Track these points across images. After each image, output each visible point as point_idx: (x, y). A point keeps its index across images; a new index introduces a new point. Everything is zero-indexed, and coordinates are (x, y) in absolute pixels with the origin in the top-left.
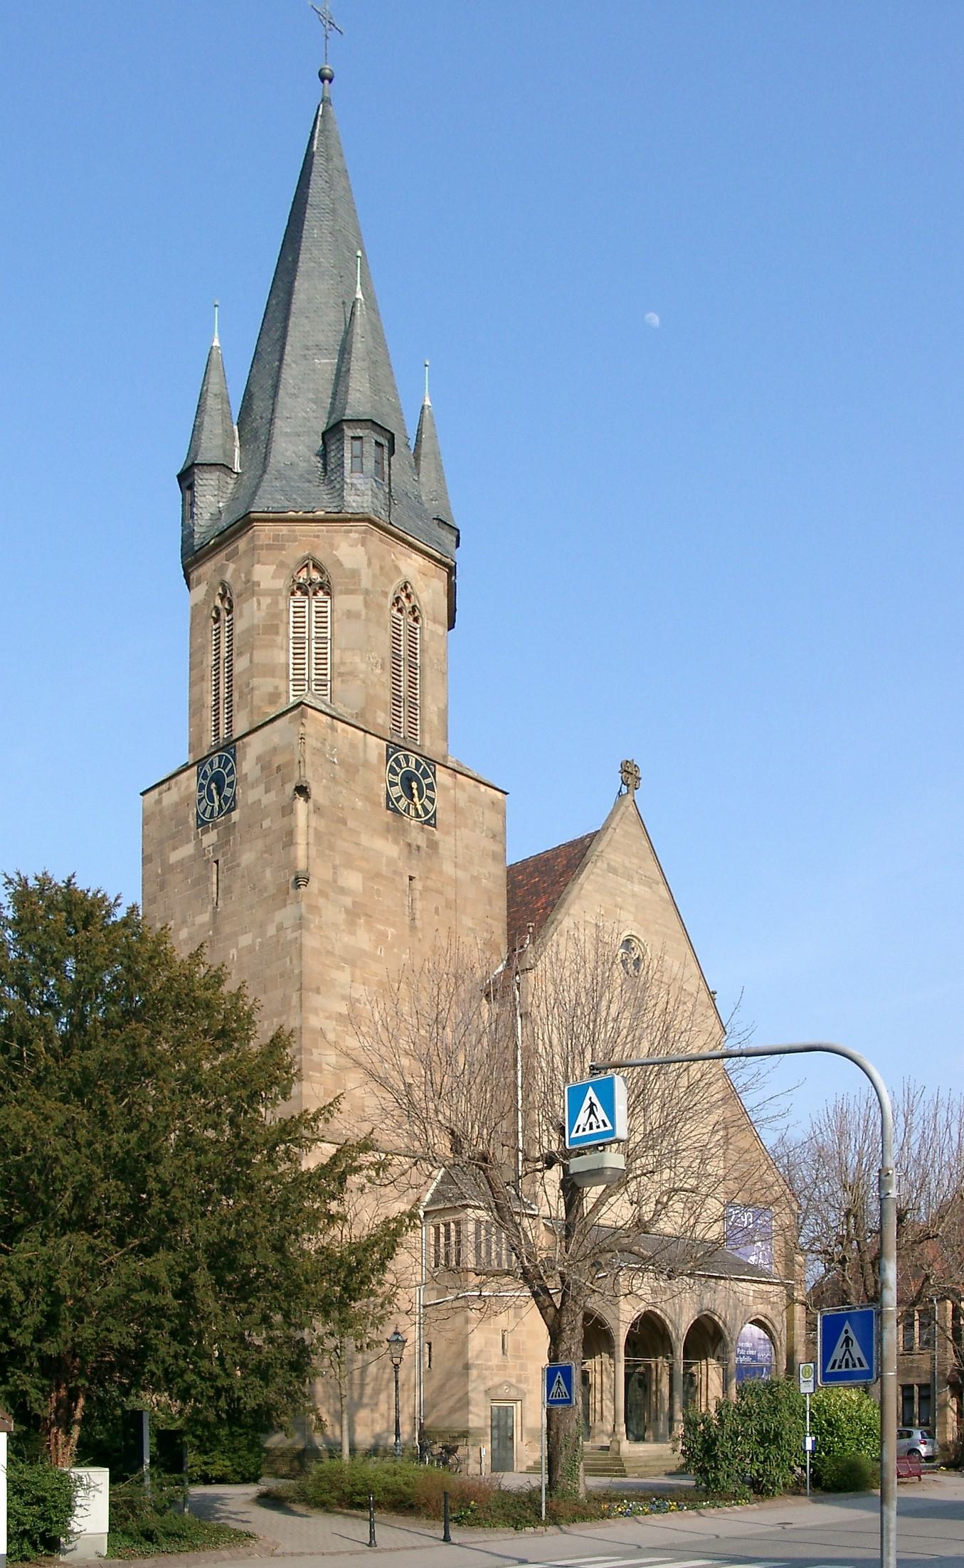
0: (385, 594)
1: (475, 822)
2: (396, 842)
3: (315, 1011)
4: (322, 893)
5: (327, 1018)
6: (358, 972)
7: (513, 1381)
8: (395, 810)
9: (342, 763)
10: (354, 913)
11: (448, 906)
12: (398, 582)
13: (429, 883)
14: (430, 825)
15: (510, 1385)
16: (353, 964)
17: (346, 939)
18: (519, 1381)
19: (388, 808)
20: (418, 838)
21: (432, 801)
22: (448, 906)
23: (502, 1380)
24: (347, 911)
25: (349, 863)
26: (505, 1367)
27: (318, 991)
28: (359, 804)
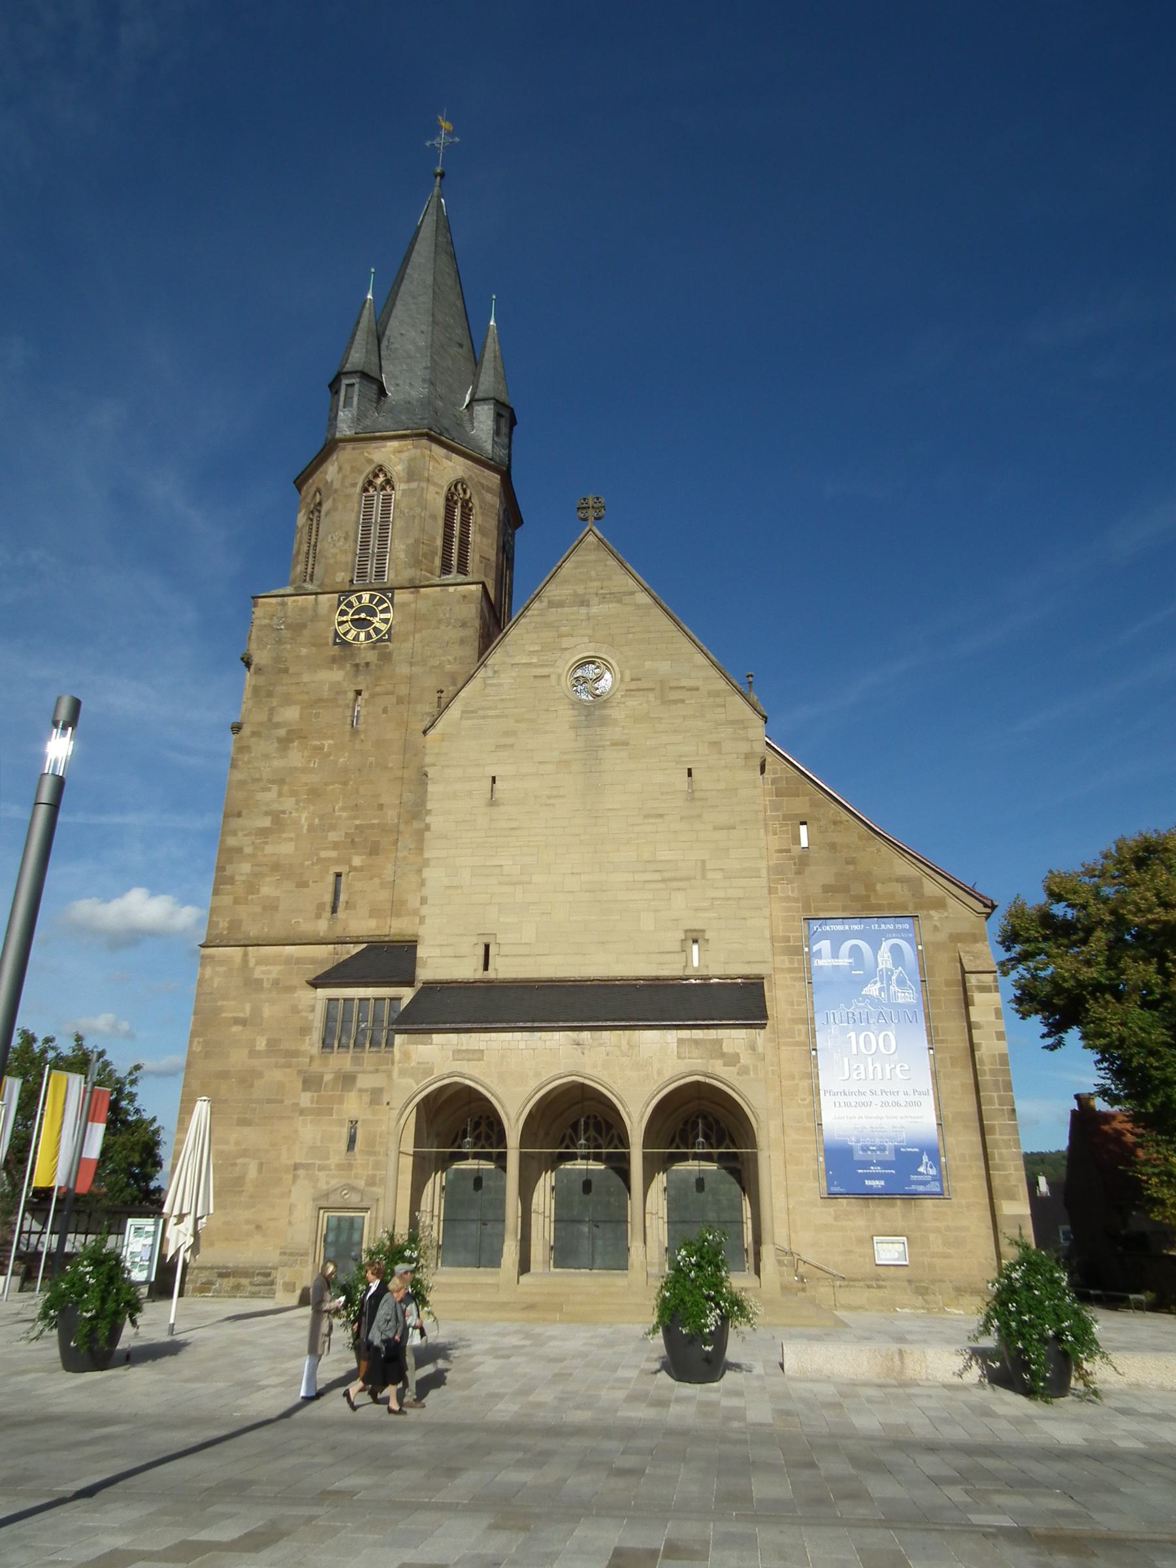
1: (440, 621)
2: (342, 667)
3: (235, 833)
5: (246, 835)
6: (286, 788)
7: (361, 1183)
8: (345, 643)
10: (284, 744)
11: (400, 701)
12: (369, 469)
13: (378, 689)
14: (384, 641)
15: (353, 1189)
16: (281, 782)
18: (371, 1182)
19: (335, 644)
21: (386, 621)
22: (400, 701)
23: (344, 1182)
24: (280, 740)
25: (287, 701)
26: (350, 1167)
27: (239, 815)
28: (304, 651)
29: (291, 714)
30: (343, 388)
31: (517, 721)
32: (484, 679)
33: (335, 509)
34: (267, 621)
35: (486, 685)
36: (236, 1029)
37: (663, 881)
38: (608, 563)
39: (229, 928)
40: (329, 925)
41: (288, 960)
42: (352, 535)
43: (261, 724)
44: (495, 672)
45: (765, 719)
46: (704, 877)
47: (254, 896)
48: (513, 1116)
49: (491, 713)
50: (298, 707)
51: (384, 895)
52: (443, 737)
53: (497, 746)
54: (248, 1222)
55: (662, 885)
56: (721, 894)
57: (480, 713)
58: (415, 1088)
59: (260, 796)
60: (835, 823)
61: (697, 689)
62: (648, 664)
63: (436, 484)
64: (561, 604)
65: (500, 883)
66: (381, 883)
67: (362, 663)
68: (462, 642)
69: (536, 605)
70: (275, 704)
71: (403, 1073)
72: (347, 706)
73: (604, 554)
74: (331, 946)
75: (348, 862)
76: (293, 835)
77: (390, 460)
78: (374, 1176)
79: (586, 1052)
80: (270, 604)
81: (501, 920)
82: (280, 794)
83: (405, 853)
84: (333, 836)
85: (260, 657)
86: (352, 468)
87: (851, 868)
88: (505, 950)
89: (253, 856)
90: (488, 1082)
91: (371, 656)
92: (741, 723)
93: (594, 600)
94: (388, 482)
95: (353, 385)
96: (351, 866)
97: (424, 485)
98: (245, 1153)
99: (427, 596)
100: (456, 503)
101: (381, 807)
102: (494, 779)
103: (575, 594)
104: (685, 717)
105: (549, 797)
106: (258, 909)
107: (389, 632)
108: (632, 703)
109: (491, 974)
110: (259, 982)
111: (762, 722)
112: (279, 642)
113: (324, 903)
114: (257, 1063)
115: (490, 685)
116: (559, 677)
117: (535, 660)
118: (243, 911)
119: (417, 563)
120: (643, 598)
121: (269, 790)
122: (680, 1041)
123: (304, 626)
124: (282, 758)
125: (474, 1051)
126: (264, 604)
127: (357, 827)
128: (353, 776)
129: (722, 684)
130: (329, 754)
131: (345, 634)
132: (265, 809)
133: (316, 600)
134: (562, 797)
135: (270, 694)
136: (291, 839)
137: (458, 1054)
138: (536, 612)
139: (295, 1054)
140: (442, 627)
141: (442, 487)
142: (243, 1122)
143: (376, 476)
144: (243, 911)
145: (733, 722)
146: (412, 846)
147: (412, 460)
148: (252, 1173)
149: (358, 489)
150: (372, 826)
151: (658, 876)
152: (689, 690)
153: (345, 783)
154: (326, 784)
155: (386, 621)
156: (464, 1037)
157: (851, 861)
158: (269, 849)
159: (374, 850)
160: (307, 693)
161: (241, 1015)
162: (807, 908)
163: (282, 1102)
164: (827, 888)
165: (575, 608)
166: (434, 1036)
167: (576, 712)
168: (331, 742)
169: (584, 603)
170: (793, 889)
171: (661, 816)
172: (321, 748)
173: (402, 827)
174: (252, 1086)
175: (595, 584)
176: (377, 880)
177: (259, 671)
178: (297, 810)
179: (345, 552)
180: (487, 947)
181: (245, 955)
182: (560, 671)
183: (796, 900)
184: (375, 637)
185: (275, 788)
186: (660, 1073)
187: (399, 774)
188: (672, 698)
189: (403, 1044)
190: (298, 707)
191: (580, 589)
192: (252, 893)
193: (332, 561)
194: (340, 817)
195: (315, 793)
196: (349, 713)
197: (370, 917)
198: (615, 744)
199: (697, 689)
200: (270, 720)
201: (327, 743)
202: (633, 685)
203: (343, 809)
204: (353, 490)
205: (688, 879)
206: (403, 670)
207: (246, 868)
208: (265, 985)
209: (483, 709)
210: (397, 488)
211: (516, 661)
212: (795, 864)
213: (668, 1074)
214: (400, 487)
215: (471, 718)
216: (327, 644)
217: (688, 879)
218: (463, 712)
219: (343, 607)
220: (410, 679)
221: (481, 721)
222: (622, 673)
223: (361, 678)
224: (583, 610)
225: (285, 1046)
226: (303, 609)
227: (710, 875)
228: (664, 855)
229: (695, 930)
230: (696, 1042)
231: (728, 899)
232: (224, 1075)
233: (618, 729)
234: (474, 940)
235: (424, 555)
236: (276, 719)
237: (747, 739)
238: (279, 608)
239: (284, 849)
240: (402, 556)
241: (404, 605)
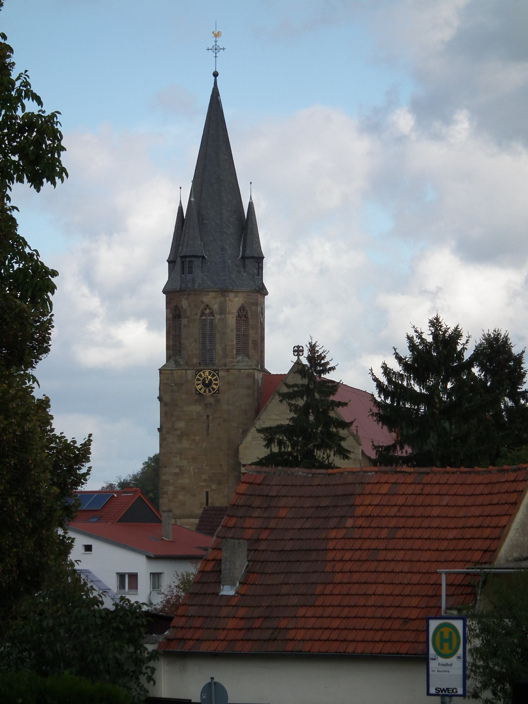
0: (196, 314)
8: (200, 393)
10: (180, 438)
12: (202, 307)
20: (211, 400)
21: (216, 384)
27: (166, 467)
28: (184, 396)
29: (181, 425)
84: (204, 477)
91: (211, 400)
101: (221, 465)
117: (278, 418)
131: (200, 389)
185: (179, 456)
201: (198, 438)
207: (171, 488)
214: (218, 317)
218: (252, 438)
219: (198, 377)
239: (185, 481)
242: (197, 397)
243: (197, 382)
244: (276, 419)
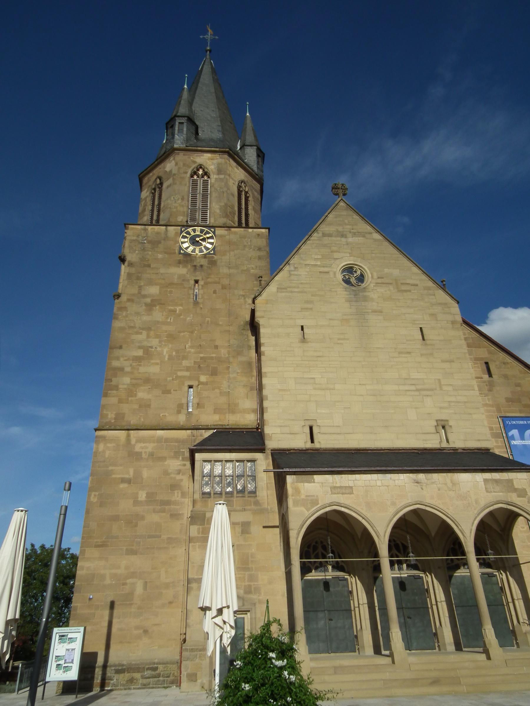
1: (245, 246)
3: (118, 358)
4: (129, 300)
5: (126, 360)
6: (152, 333)
9: (149, 242)
11: (224, 287)
12: (195, 166)
13: (209, 280)
16: (149, 329)
17: (145, 318)
20: (204, 262)
24: (146, 305)
25: (151, 283)
27: (121, 347)
28: (160, 256)
29: (154, 290)
30: (177, 123)
31: (312, 295)
32: (290, 271)
33: (174, 184)
34: (135, 238)
35: (290, 275)
36: (122, 486)
37: (417, 390)
38: (354, 217)
39: (115, 419)
40: (187, 418)
41: (159, 440)
42: (186, 197)
43: (134, 295)
44: (295, 268)
45: (458, 303)
46: (441, 389)
47: (133, 398)
48: (382, 534)
49: (296, 290)
50: (158, 287)
51: (223, 400)
52: (267, 302)
53: (302, 309)
54: (137, 628)
55: (417, 393)
56: (453, 399)
57: (288, 289)
58: (307, 514)
59: (134, 337)
60: (504, 363)
61: (417, 285)
62: (386, 270)
63: (233, 179)
64: (330, 235)
65: (315, 389)
66: (221, 393)
67: (198, 265)
68: (260, 258)
69: (315, 234)
70: (142, 284)
71: (296, 503)
72: (190, 288)
73: (351, 213)
74: (190, 431)
75: (198, 379)
76: (158, 361)
77: (207, 163)
78: (250, 586)
79: (424, 487)
80: (136, 229)
81: (318, 411)
82: (148, 336)
83: (235, 375)
85: (130, 257)
86: (184, 165)
87: (519, 389)
88: (323, 430)
89: (132, 373)
90: (359, 509)
91: (204, 262)
92: (445, 305)
93: (350, 235)
94: (206, 173)
95: (183, 123)
96: (199, 381)
97: (228, 177)
98: (133, 575)
99: (235, 233)
100: (242, 191)
101: (216, 347)
102: (302, 328)
103: (338, 231)
104: (413, 300)
105: (339, 339)
106: (136, 406)
107: (214, 249)
108: (381, 290)
109: (317, 445)
110: (139, 454)
111: (457, 305)
112: (144, 250)
113: (182, 404)
114: (139, 509)
115: (294, 275)
116: (335, 273)
117: (319, 263)
118: (125, 408)
119: (226, 216)
120: (377, 236)
121: (141, 333)
122: (486, 481)
123: (159, 242)
124: (149, 315)
125: (346, 487)
126: (133, 229)
127: (202, 358)
128: (197, 328)
129: (430, 284)
130: (180, 315)
132: (138, 344)
133: (166, 229)
134: (348, 339)
135: (138, 278)
136: (157, 364)
137: (335, 489)
138: (316, 238)
139: (168, 503)
140: (247, 249)
141: (236, 181)
142: (131, 552)
143: (198, 170)
144: (125, 408)
145: (440, 304)
146: (239, 371)
147: (219, 164)
148: (139, 590)
149: (188, 175)
150: (212, 358)
151: (413, 388)
152: (412, 285)
153: (192, 332)
154: (180, 332)
155: (212, 244)
156: (337, 477)
157: (518, 385)
158: (142, 369)
159: (214, 373)
160: (164, 279)
161: (127, 476)
162: (499, 410)
163: (160, 537)
164: (508, 400)
165: (339, 238)
166: (315, 477)
167: (348, 293)
168: (180, 307)
169: (343, 236)
170: (489, 399)
171: (409, 353)
172: (175, 311)
173: (231, 359)
174: (136, 525)
175: (349, 227)
176: (217, 391)
177: (131, 265)
178: (160, 346)
179: (183, 206)
180: (311, 428)
181: (128, 436)
182: (335, 270)
183: (492, 406)
184: (205, 252)
185: (145, 333)
186: (477, 502)
187: (227, 328)
188: (403, 289)
189: (293, 483)
190: (158, 287)
191: (340, 229)
192: (132, 396)
193: (174, 210)
194: (190, 352)
195: (172, 337)
196: (191, 292)
197: (215, 413)
198: (374, 311)
199: (417, 285)
200: (139, 293)
201: (178, 309)
202: (380, 281)
203: (191, 347)
204: (185, 175)
205: (432, 390)
206: (225, 270)
207: (127, 380)
208: (144, 456)
209: (290, 287)
210: (212, 176)
211: (308, 262)
212: (487, 385)
213: (483, 503)
214: (214, 177)
215: (283, 292)
216: (175, 253)
217: (432, 390)
218: (278, 288)
220: (230, 275)
221: (290, 294)
222: (372, 274)
223: (197, 273)
224: (343, 240)
225: (160, 497)
226: (158, 233)
227: (445, 388)
228: (415, 375)
229: (442, 420)
230: (497, 481)
231: (458, 402)
232: (116, 518)
233: (374, 303)
234: (303, 423)
235: (230, 213)
236: (143, 292)
237: (451, 314)
238: (143, 231)
239: (152, 369)
240: (218, 211)
241: (221, 236)
242: (181, 257)
243: (183, 240)
244: (316, 265)
